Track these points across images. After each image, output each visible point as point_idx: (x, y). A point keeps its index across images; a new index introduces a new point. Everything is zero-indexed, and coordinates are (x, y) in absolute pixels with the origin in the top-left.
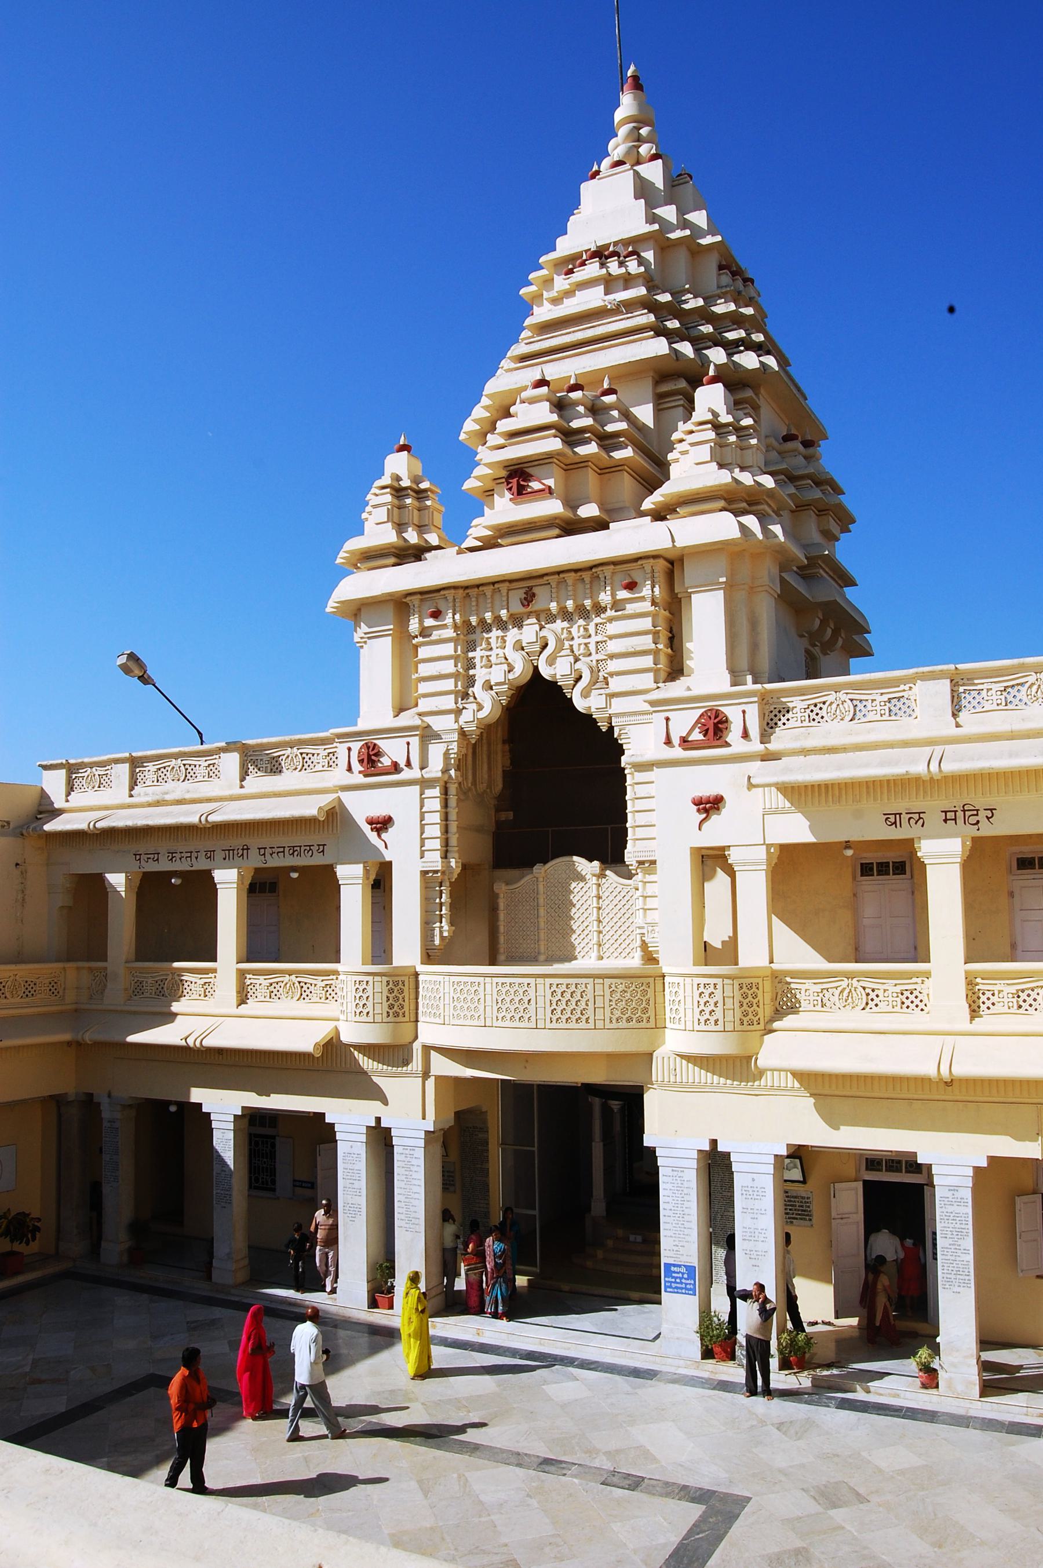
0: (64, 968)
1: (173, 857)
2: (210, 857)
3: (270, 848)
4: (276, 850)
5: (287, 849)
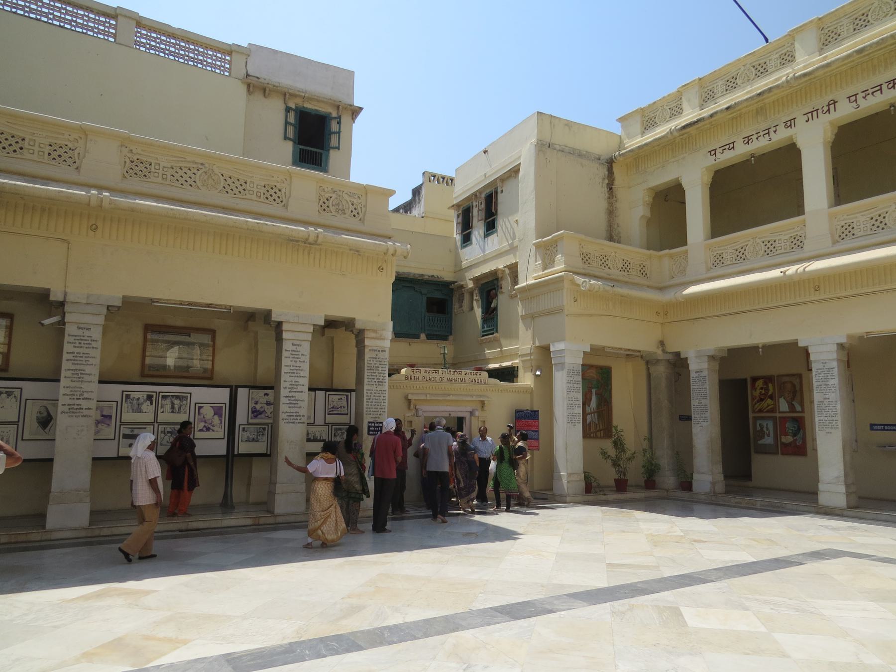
0: (651, 255)
1: (749, 140)
2: (791, 125)
4: (870, 91)
5: (884, 87)
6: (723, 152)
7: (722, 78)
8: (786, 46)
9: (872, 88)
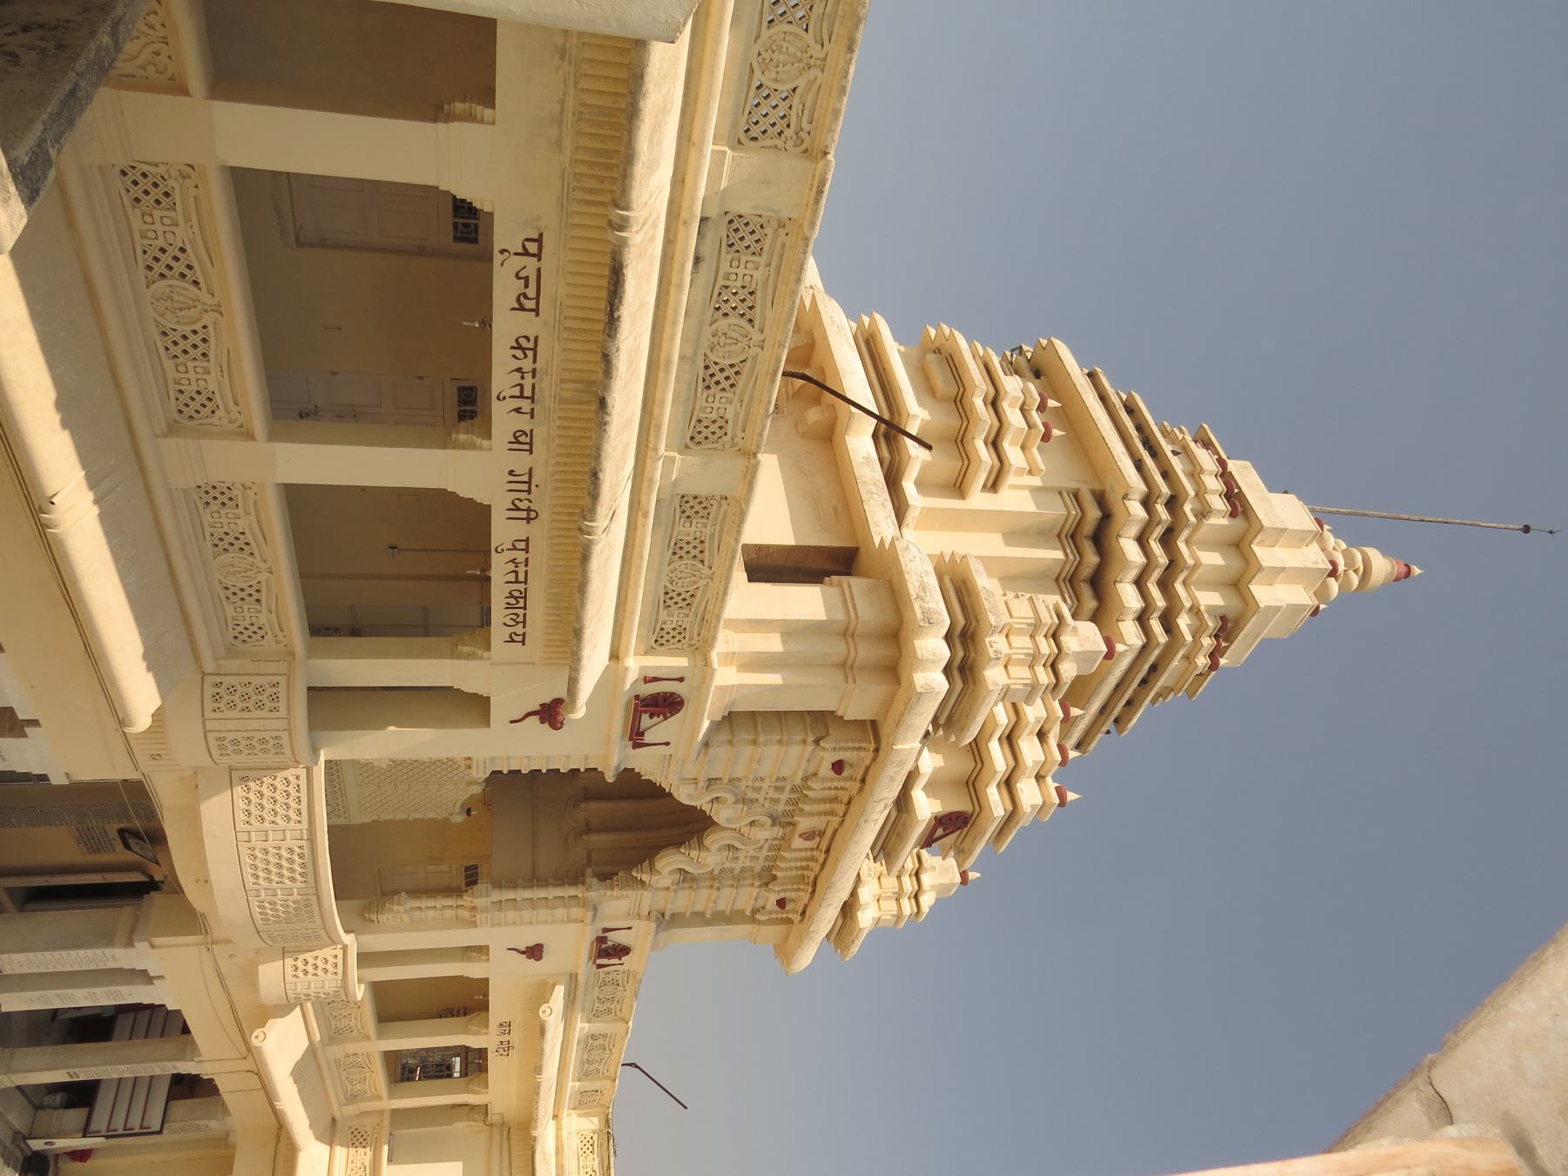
1: (524, 350)
3: (527, 559)
4: (521, 569)
5: (521, 587)
6: (518, 277)
7: (771, 283)
8: (741, 435)
9: (526, 572)
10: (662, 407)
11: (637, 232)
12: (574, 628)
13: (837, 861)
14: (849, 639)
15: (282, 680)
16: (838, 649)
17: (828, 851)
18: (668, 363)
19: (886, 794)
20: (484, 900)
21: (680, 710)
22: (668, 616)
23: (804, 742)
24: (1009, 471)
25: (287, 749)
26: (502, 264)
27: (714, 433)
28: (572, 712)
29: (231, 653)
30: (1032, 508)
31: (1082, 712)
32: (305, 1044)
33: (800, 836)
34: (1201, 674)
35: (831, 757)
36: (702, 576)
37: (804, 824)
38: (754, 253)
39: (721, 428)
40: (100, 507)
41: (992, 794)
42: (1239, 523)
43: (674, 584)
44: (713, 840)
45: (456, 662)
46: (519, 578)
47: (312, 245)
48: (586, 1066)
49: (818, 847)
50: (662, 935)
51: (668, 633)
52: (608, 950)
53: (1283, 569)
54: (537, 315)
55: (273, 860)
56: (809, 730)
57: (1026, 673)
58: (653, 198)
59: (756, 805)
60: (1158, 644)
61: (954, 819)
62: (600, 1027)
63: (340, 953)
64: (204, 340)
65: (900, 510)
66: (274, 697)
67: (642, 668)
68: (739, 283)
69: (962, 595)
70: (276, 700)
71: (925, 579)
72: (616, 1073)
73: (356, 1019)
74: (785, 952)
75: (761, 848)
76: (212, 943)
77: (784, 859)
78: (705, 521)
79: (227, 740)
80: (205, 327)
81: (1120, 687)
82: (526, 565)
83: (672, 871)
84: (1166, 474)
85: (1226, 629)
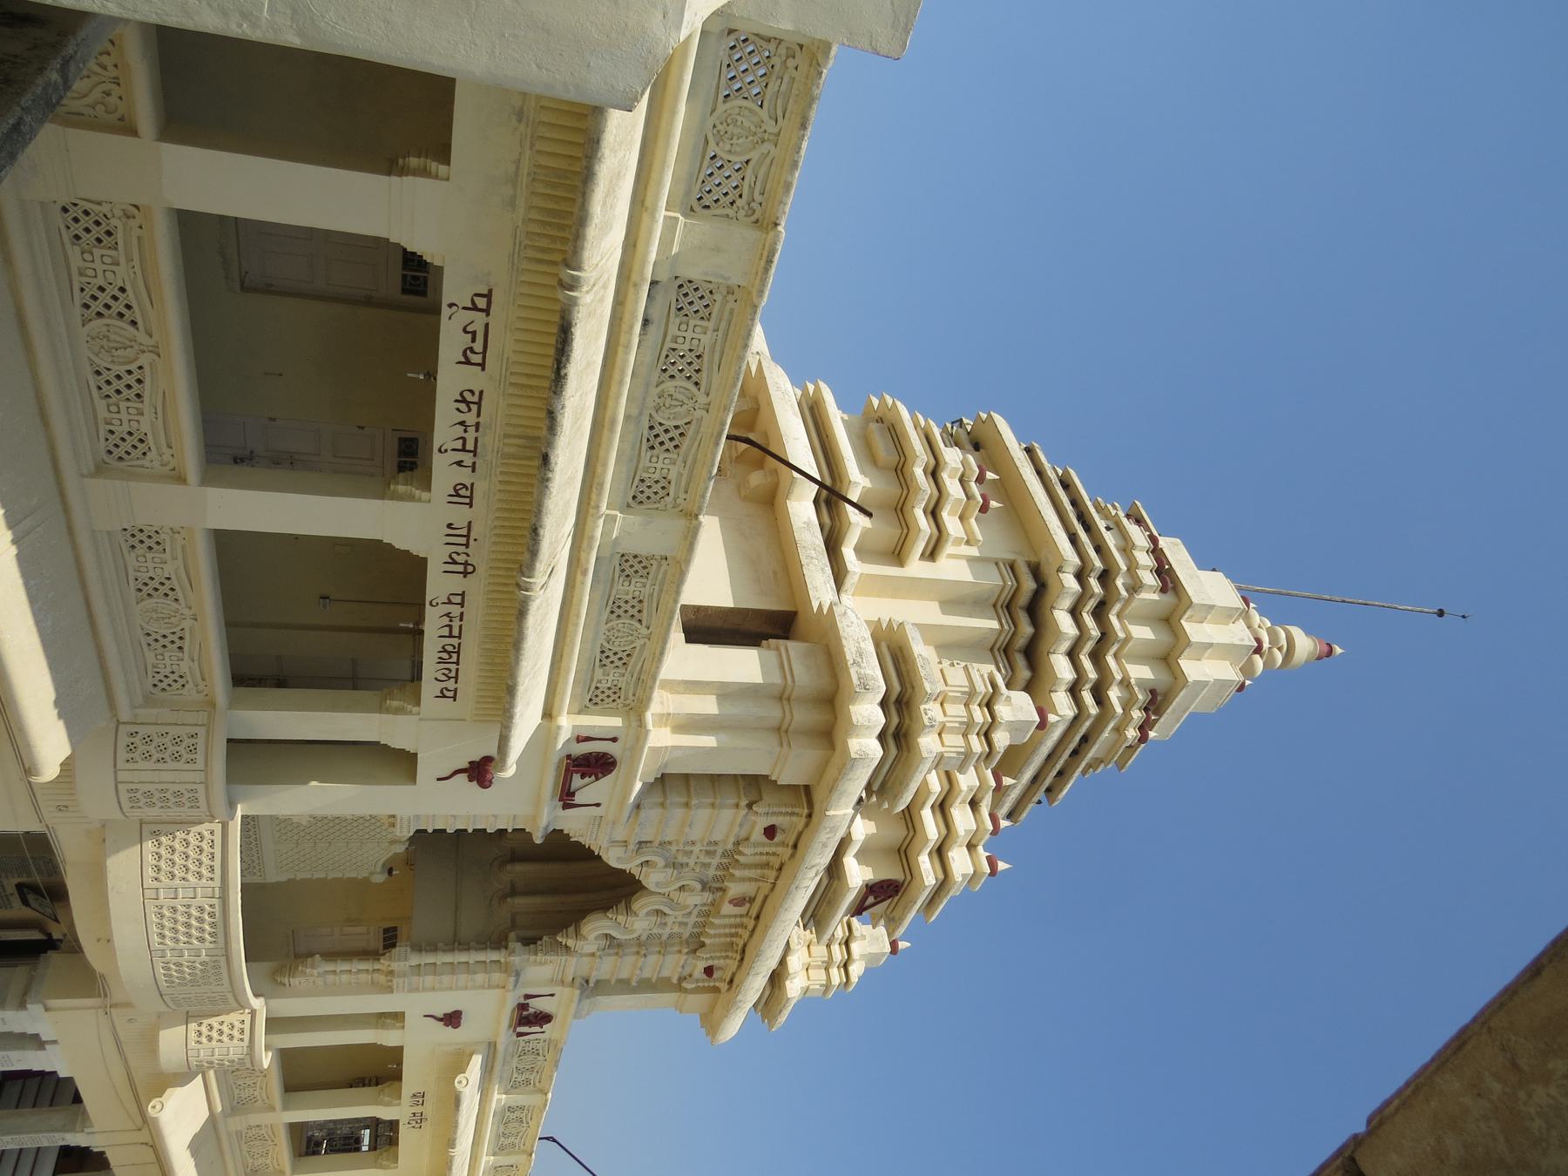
1: (468, 403)
2: (459, 495)
3: (462, 614)
4: (456, 624)
5: (455, 641)
6: (465, 331)
7: (718, 348)
9: (461, 627)
10: (605, 465)
11: (587, 292)
12: (507, 684)
13: (767, 928)
14: (785, 702)
15: (201, 731)
16: (773, 713)
17: (758, 917)
18: (613, 422)
19: (817, 861)
20: (402, 964)
21: (612, 771)
22: (603, 675)
23: (737, 806)
24: (947, 540)
25: (202, 802)
26: (450, 318)
27: (656, 493)
28: (501, 770)
29: (149, 701)
30: (969, 578)
31: (1014, 781)
32: (204, 1114)
33: (730, 902)
34: (1130, 746)
35: (764, 822)
36: (640, 636)
37: (735, 890)
38: (702, 318)
39: (663, 488)
40: (18, 548)
41: (924, 862)
42: (1169, 598)
43: (611, 643)
44: (642, 905)
45: (385, 716)
46: (453, 632)
47: (256, 290)
48: (502, 1139)
49: (747, 914)
50: (586, 1003)
51: (603, 692)
52: (529, 1018)
53: (1211, 645)
54: (483, 369)
55: (181, 919)
56: (742, 793)
57: (959, 741)
58: (604, 261)
59: (686, 870)
60: (1089, 715)
61: (885, 887)
62: (518, 1099)
63: (248, 1019)
64: (139, 381)
65: (839, 575)
66: (192, 748)
67: (574, 727)
68: (686, 346)
69: (899, 663)
70: (194, 751)
71: (862, 645)
72: (532, 1147)
73: (262, 1089)
74: (711, 1023)
75: (690, 913)
76: (110, 1007)
77: (713, 925)
78: (645, 580)
79: (140, 792)
80: (140, 368)
81: (1051, 757)
82: (461, 620)
83: (598, 936)
84: (1100, 549)
85: (1156, 703)
